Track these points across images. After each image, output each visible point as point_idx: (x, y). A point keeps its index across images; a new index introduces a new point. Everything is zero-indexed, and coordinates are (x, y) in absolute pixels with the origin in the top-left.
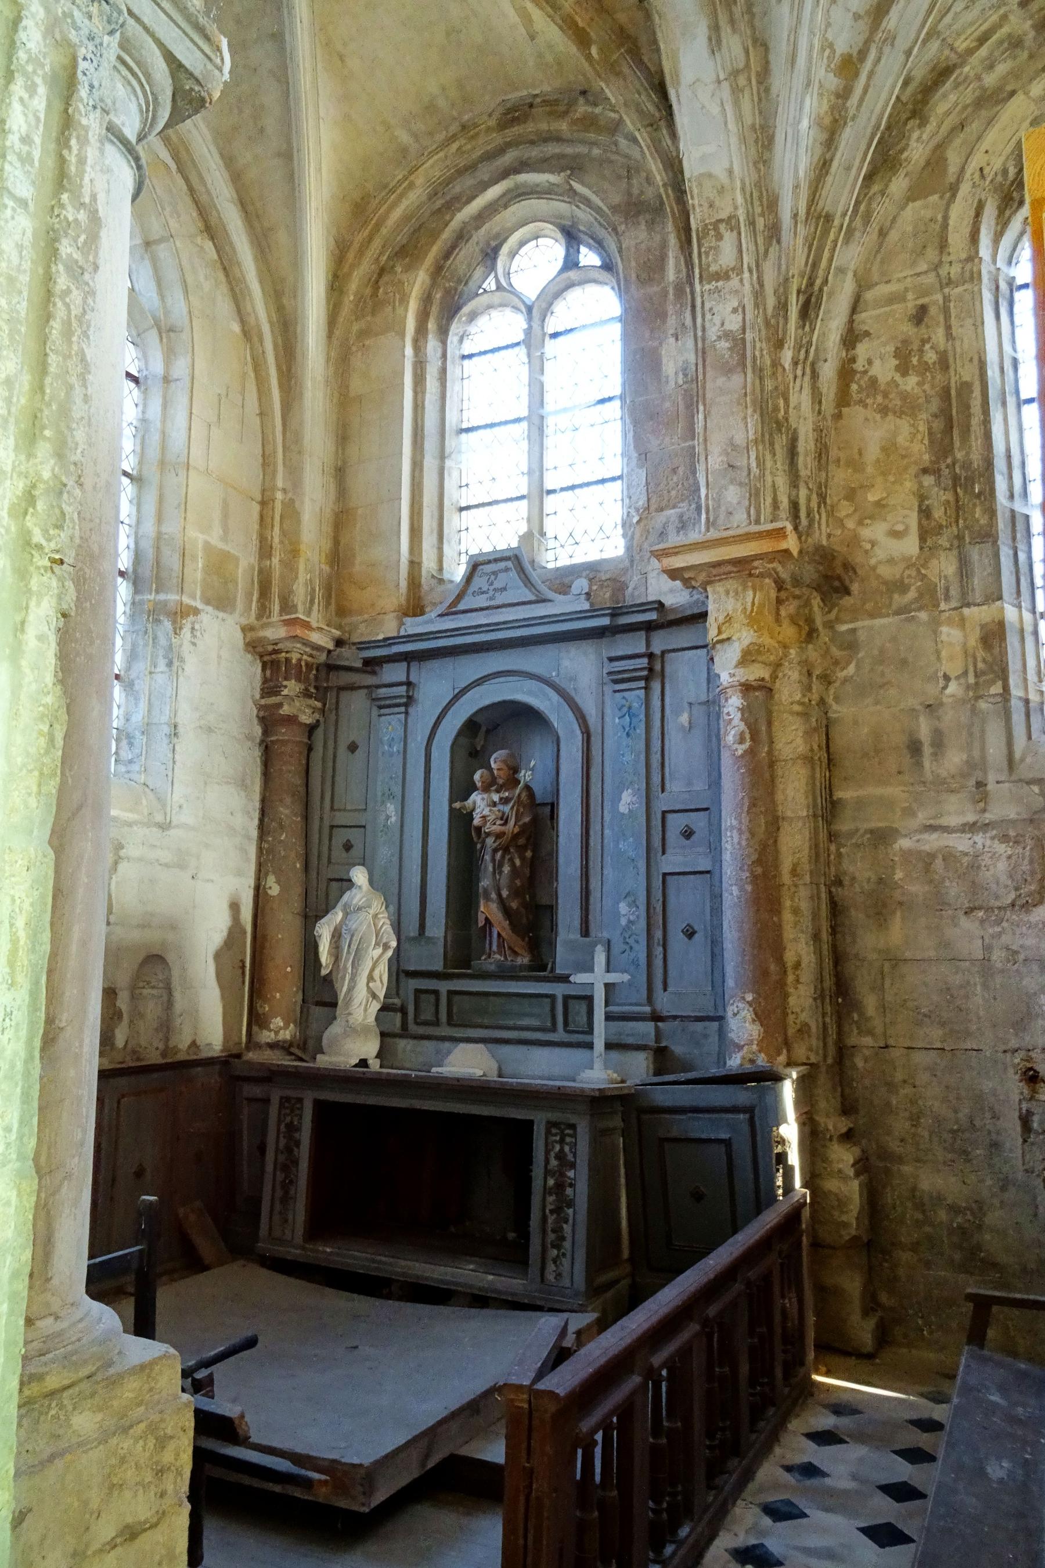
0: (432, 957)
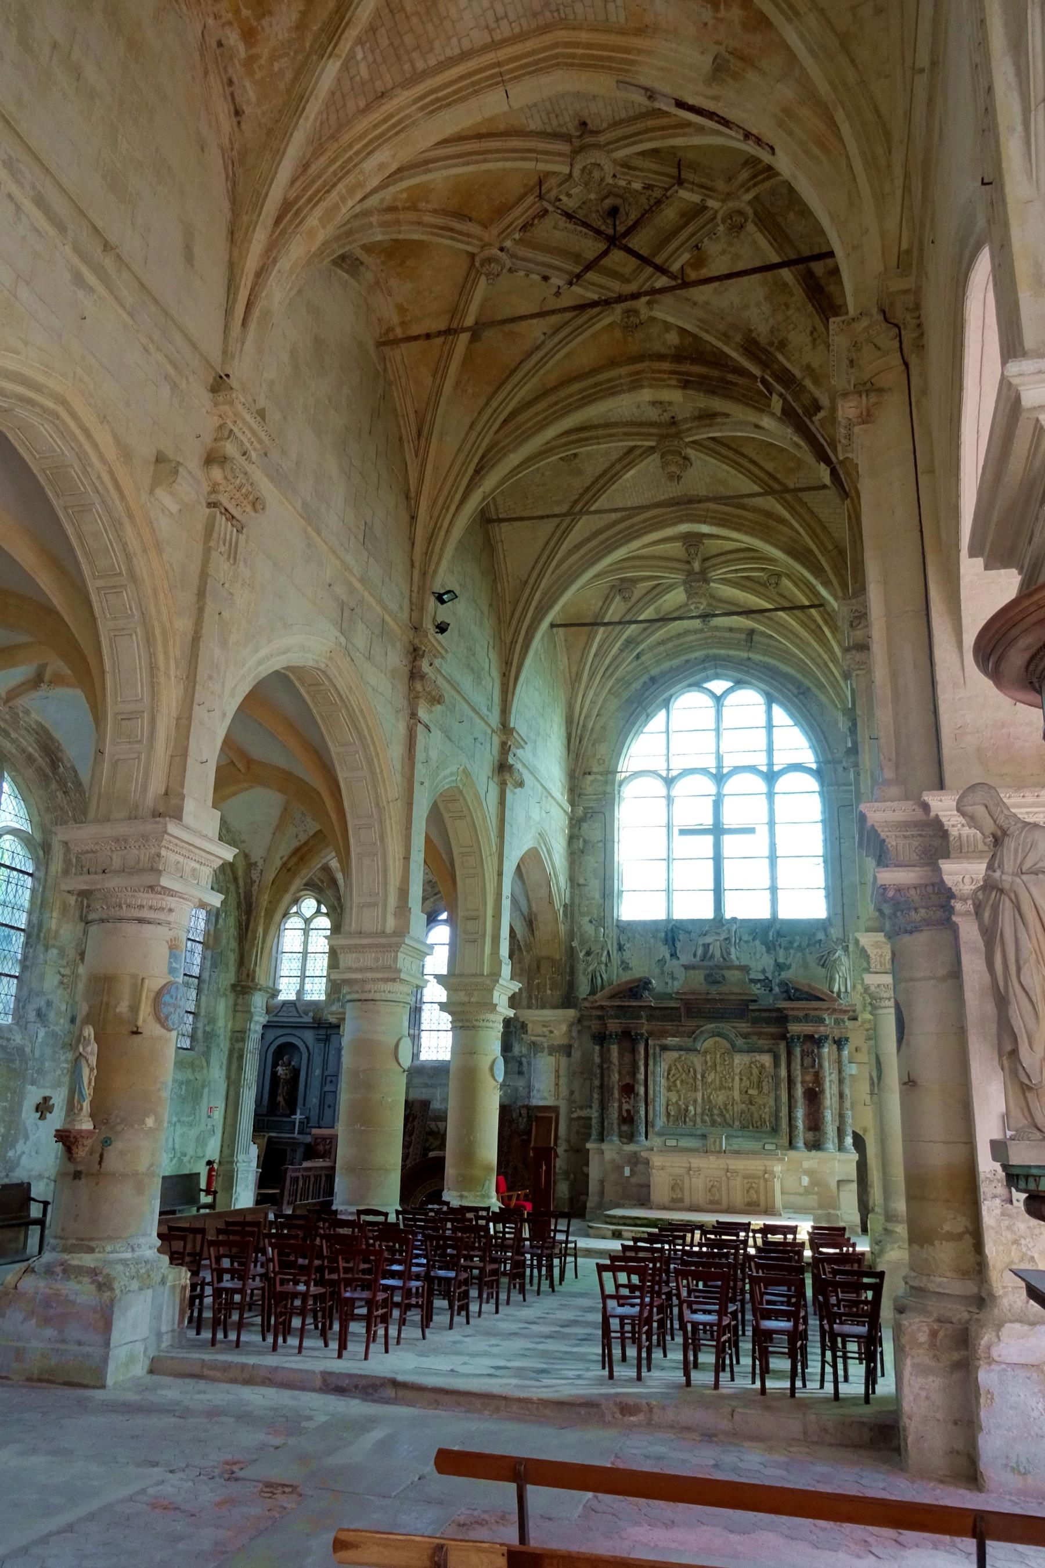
0: (264, 1110)
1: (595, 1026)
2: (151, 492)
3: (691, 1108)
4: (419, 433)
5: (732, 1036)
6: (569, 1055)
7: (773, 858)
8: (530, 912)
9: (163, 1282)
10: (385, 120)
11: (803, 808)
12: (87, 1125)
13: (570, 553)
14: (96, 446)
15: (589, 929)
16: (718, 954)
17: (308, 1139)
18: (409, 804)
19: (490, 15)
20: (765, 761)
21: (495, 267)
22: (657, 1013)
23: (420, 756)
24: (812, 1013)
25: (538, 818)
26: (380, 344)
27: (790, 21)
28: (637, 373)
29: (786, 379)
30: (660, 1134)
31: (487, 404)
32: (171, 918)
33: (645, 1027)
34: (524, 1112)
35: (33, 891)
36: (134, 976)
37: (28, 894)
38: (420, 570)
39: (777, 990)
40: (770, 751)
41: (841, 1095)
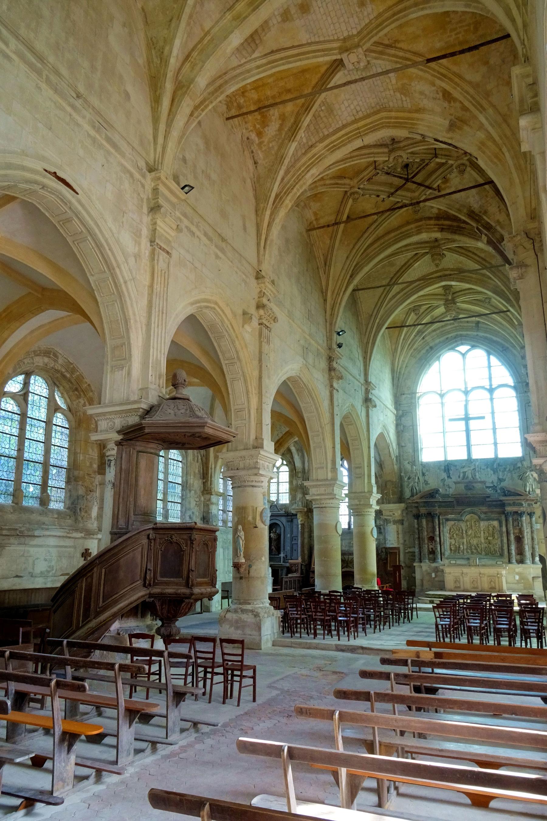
1: (415, 511)
2: (243, 327)
3: (461, 546)
4: (325, 264)
5: (479, 513)
6: (403, 524)
7: (494, 429)
8: (381, 460)
9: (273, 615)
10: (313, 157)
11: (508, 404)
12: (243, 560)
13: (391, 299)
14: (226, 315)
15: (408, 467)
16: (470, 476)
17: (288, 565)
18: (333, 424)
19: (354, 111)
20: (488, 384)
21: (356, 196)
22: (443, 504)
23: (336, 403)
24: (517, 502)
25: (383, 420)
26: (308, 230)
27: (481, 112)
28: (419, 226)
29: (488, 227)
30: (447, 558)
31: (353, 247)
32: (263, 484)
33: (437, 510)
34: (384, 550)
35: (182, 468)
36: (253, 507)
37: (180, 470)
38: (330, 322)
39: (499, 491)
40: (490, 379)
41: (533, 539)
